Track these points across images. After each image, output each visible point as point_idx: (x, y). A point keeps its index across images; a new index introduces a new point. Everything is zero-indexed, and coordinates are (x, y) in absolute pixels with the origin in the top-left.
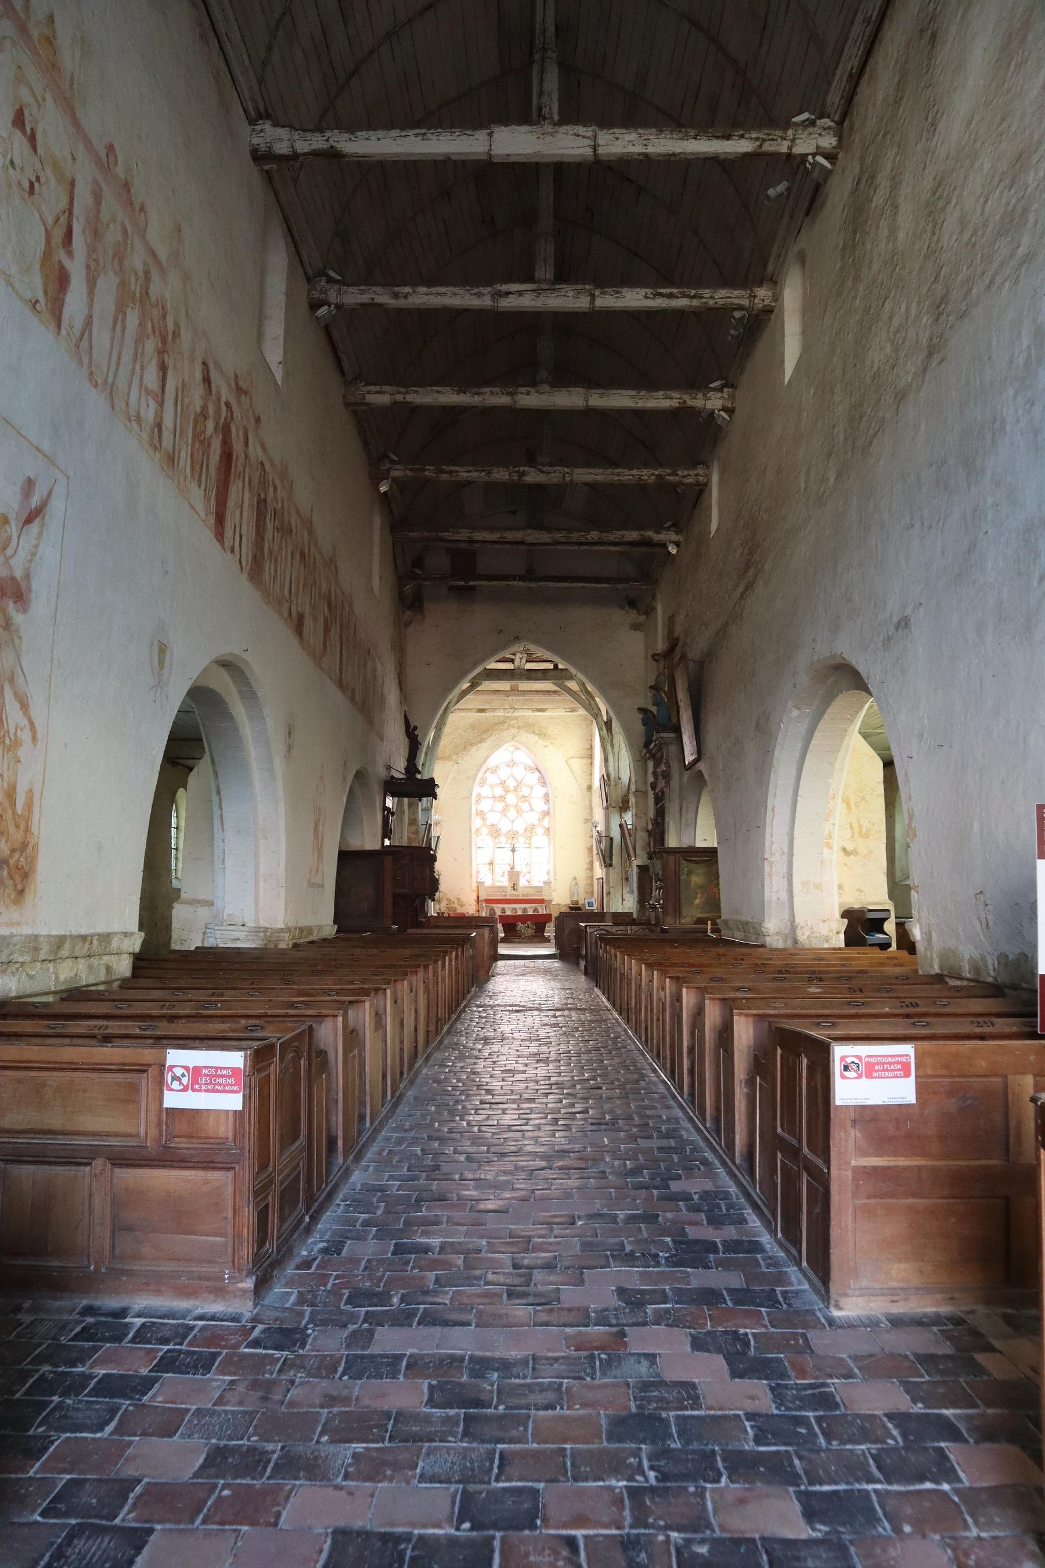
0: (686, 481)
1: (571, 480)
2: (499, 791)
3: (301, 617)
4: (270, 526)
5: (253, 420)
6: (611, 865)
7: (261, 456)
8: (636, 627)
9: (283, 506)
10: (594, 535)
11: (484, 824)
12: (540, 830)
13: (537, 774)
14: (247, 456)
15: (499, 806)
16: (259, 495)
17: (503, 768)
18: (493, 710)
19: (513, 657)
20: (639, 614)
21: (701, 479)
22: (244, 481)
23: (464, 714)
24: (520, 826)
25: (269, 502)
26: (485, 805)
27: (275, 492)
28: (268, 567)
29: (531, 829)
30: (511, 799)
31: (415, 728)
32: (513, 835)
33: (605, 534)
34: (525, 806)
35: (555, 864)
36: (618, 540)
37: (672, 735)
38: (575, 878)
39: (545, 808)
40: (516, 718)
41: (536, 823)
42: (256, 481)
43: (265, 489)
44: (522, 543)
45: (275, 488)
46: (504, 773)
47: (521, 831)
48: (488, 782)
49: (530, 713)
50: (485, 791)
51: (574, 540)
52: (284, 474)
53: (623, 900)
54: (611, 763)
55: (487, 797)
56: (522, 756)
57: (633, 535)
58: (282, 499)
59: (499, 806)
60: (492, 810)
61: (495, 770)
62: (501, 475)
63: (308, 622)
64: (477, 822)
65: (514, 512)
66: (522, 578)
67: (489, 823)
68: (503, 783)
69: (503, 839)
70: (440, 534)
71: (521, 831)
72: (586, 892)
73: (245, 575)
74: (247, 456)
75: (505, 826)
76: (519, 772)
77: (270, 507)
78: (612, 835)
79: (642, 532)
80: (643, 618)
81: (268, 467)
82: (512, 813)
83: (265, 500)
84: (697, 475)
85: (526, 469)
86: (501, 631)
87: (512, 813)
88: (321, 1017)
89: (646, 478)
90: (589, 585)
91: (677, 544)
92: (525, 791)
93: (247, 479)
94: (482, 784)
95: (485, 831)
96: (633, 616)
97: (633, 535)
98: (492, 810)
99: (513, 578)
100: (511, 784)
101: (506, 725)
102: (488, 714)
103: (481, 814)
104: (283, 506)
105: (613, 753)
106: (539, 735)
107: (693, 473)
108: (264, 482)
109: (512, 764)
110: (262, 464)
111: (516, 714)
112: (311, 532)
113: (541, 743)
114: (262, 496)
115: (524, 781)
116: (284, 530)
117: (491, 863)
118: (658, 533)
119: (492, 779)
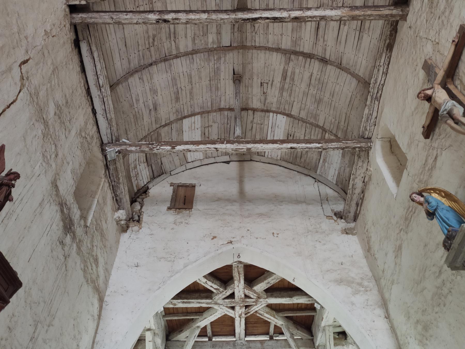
8: (346, 232)
20: (347, 222)
65: (228, 162)
80: (352, 225)
86: (214, 237)
90: (299, 145)
96: (342, 224)
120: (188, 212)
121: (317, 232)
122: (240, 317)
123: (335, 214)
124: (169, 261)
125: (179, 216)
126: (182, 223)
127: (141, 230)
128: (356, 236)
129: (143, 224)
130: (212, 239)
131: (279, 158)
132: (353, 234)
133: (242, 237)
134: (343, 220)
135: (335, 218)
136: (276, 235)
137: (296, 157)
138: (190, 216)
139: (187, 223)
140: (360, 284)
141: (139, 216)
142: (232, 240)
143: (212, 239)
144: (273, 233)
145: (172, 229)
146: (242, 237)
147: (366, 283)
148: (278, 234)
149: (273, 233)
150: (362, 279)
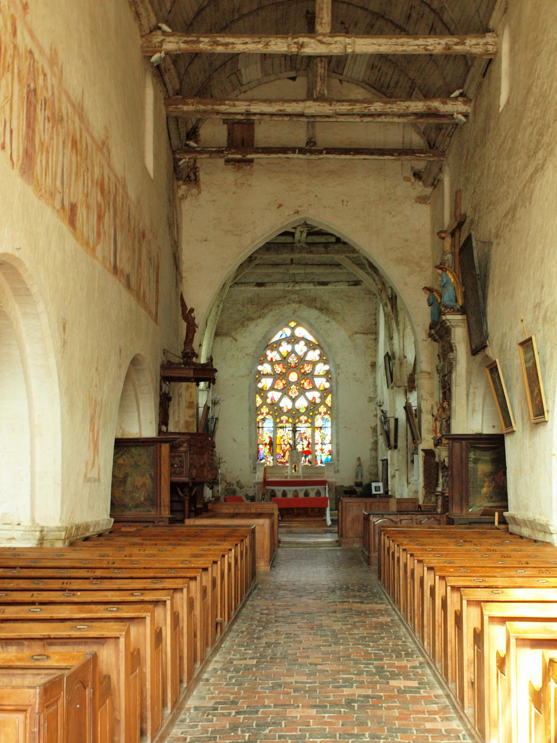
0: (475, 50)
1: (353, 52)
2: (279, 369)
3: (73, 207)
4: (40, 116)
5: (20, 7)
6: (396, 447)
7: (30, 44)
8: (422, 200)
9: (53, 94)
10: (377, 107)
11: (264, 403)
12: (322, 409)
13: (318, 352)
14: (15, 47)
15: (280, 385)
16: (29, 86)
17: (284, 344)
18: (274, 283)
19: (293, 231)
20: (425, 185)
21: (490, 48)
22: (13, 73)
23: (243, 288)
24: (302, 404)
25: (39, 91)
26: (266, 383)
27: (45, 80)
28: (40, 160)
29: (313, 407)
30: (293, 377)
31: (192, 310)
33: (389, 106)
35: (337, 445)
36: (402, 111)
37: (459, 317)
38: (359, 459)
39: (327, 385)
40: (297, 292)
41: (318, 401)
42: (25, 72)
43: (35, 80)
44: (302, 115)
45: (45, 75)
46: (285, 348)
47: (302, 410)
48: (269, 358)
49: (311, 287)
50: (266, 368)
51: (356, 111)
52: (53, 60)
53: (408, 483)
54: (396, 341)
55: (267, 375)
56: (301, 332)
57: (418, 106)
58: (52, 86)
60: (272, 388)
62: (279, 46)
63: (81, 212)
64: (259, 401)
65: (293, 79)
66: (302, 151)
67: (269, 401)
68: (284, 359)
69: (284, 418)
70: (216, 107)
71: (302, 410)
72: (371, 474)
73: (16, 171)
74: (15, 47)
75: (286, 404)
76: (300, 348)
77: (40, 97)
78: (397, 416)
79: (428, 103)
80: (429, 190)
81: (37, 56)
82: (294, 392)
83: (35, 90)
84: (486, 44)
85: (306, 40)
86: (280, 206)
87: (294, 392)
88: (101, 640)
89: (431, 48)
91: (466, 116)
92: (308, 368)
93: (16, 71)
95: (265, 410)
96: (419, 188)
97: (418, 106)
98: (272, 388)
99: (293, 150)
100: (292, 360)
101: (287, 299)
102: (268, 289)
103: (262, 392)
104: (53, 94)
105: (398, 330)
106: (321, 310)
107: (482, 41)
108: (33, 72)
109: (293, 340)
110: (31, 52)
111: (297, 288)
112: (82, 117)
113: (324, 318)
114: (32, 86)
115: (308, 358)
116: (56, 119)
117: (271, 444)
118: (444, 103)
119: (272, 355)
120: (249, 167)
121: (390, 199)
122: (302, 232)
123: (415, 175)
124: (236, 235)
125: (239, 175)
126: (244, 184)
127: (200, 195)
128: (429, 206)
129: (202, 186)
130: (278, 207)
131: (361, 79)
132: (425, 203)
133: (310, 205)
134: (421, 183)
135: (413, 179)
136: (345, 203)
137: (382, 86)
138: (252, 175)
139: (250, 185)
140: (418, 264)
141: (195, 174)
142: (299, 209)
143: (278, 207)
144: (343, 201)
145: (234, 193)
146: (310, 205)
147: (423, 263)
148: (348, 202)
149: (343, 201)
150: (422, 258)
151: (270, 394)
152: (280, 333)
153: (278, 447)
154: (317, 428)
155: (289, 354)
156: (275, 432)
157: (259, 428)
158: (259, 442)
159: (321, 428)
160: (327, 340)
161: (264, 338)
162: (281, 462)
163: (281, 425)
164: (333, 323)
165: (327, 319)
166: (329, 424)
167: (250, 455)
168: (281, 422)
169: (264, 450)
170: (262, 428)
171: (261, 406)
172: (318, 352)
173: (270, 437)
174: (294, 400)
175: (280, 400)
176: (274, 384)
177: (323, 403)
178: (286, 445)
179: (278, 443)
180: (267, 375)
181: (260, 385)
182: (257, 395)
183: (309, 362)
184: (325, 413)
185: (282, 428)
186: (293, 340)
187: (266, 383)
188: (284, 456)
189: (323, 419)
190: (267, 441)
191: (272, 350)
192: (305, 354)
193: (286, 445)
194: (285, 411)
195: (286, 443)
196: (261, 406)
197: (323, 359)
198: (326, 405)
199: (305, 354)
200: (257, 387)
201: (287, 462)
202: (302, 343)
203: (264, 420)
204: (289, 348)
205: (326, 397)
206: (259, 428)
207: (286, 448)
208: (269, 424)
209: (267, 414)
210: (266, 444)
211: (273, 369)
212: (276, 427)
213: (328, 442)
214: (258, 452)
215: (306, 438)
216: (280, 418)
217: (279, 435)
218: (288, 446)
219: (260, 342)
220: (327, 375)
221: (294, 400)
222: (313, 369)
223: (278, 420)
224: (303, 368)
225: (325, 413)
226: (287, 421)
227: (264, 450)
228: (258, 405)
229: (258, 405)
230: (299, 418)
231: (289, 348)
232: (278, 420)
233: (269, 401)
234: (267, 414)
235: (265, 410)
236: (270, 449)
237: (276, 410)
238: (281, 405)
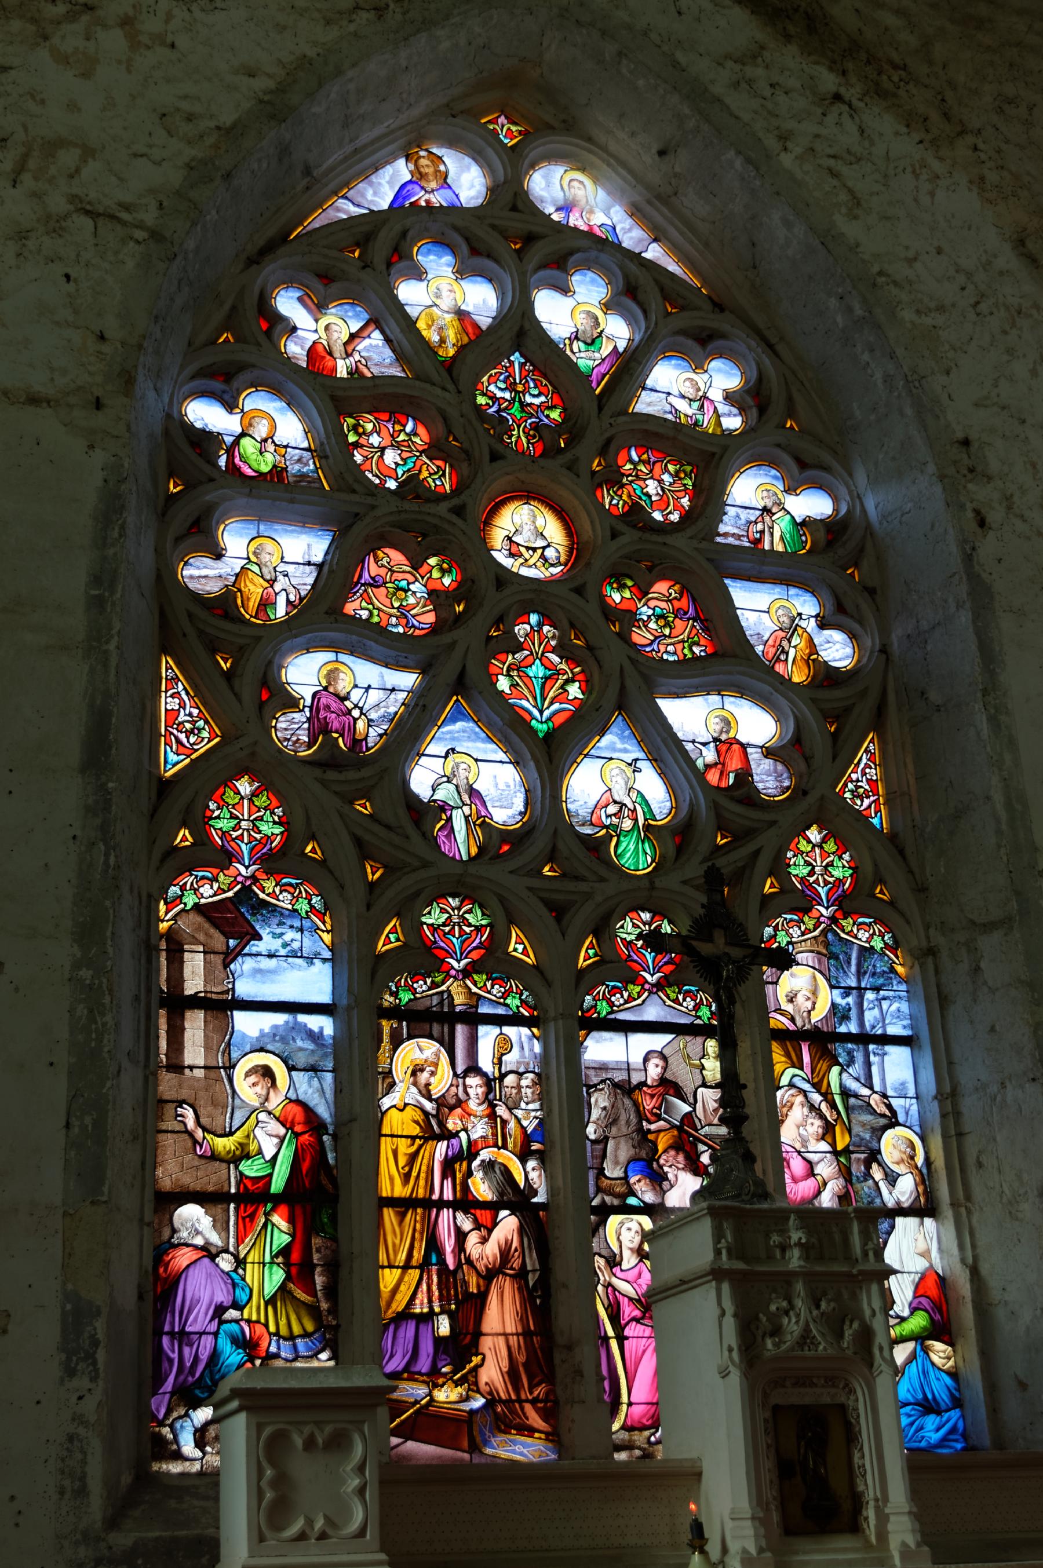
11: (244, 749)
12: (816, 860)
15: (404, 590)
32: (547, 869)
34: (657, 620)
41: (768, 779)
46: (443, 295)
50: (273, 430)
59: (404, 590)
60: (324, 615)
61: (366, 262)
64: (183, 725)
68: (433, 383)
71: (635, 856)
75: (472, 776)
92: (658, 489)
94: (248, 353)
95: (247, 815)
98: (324, 615)
151: (303, 673)
152: (401, 170)
153: (398, 1236)
154: (782, 1036)
155: (483, 345)
156: (358, 1072)
157: (178, 1003)
158: (172, 1170)
159: (822, 1042)
160: (851, 230)
161: (275, 108)
162: (428, 1423)
163: (409, 992)
164: (883, 123)
165: (829, 81)
166: (892, 1012)
167: (76, 1316)
168: (423, 956)
169: (233, 1273)
170: (222, 1006)
171: (210, 775)
172: (723, 378)
173: (302, 1121)
174: (547, 756)
175: (410, 731)
176: (335, 579)
177: (814, 799)
178: (484, 1216)
179: (391, 1183)
180: (276, 495)
181: (201, 574)
182: (167, 666)
183: (668, 438)
184: (846, 903)
185: (437, 1021)
186: (515, 242)
187: (274, 558)
188: (461, 1350)
189: (832, 955)
190: (271, 1151)
191: (323, 289)
192: (629, 368)
193: (484, 1216)
194: (462, 842)
195: (482, 1189)
196: (210, 775)
197: (788, 426)
198: (844, 827)
199: (629, 368)
200: (166, 585)
201: (502, 1417)
202: (590, 290)
203: (234, 923)
204: (481, 299)
205: (842, 755)
206: (178, 1003)
207: (484, 1251)
208: (290, 970)
209: (274, 861)
210: (254, 1197)
211: (332, 449)
212: (369, 1014)
213: (905, 1189)
214: (162, 1289)
215: (685, 1141)
216: (408, 911)
217: (400, 1107)
218: (508, 1224)
219: (231, 133)
220: (833, 563)
221: (547, 756)
222: (709, 500)
223: (389, 938)
224: (614, 479)
225: (846, 903)
226: (492, 961)
227: (233, 1273)
228: (172, 761)
229: (172, 761)
230: (602, 930)
231: (481, 299)
232: (389, 938)
233: (290, 728)
234: (274, 861)
235: (247, 815)
236: (295, 1262)
237: (357, 830)
238: (422, 779)
